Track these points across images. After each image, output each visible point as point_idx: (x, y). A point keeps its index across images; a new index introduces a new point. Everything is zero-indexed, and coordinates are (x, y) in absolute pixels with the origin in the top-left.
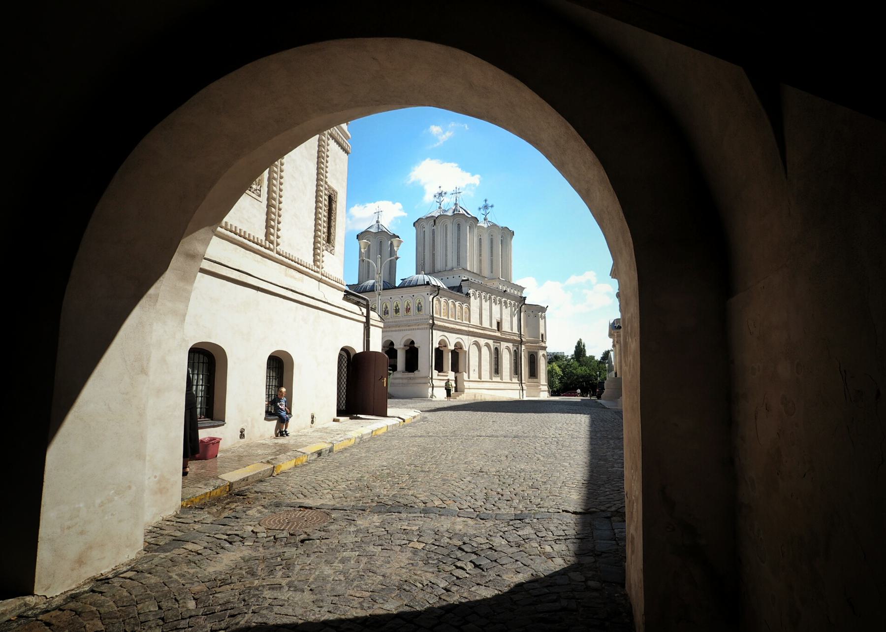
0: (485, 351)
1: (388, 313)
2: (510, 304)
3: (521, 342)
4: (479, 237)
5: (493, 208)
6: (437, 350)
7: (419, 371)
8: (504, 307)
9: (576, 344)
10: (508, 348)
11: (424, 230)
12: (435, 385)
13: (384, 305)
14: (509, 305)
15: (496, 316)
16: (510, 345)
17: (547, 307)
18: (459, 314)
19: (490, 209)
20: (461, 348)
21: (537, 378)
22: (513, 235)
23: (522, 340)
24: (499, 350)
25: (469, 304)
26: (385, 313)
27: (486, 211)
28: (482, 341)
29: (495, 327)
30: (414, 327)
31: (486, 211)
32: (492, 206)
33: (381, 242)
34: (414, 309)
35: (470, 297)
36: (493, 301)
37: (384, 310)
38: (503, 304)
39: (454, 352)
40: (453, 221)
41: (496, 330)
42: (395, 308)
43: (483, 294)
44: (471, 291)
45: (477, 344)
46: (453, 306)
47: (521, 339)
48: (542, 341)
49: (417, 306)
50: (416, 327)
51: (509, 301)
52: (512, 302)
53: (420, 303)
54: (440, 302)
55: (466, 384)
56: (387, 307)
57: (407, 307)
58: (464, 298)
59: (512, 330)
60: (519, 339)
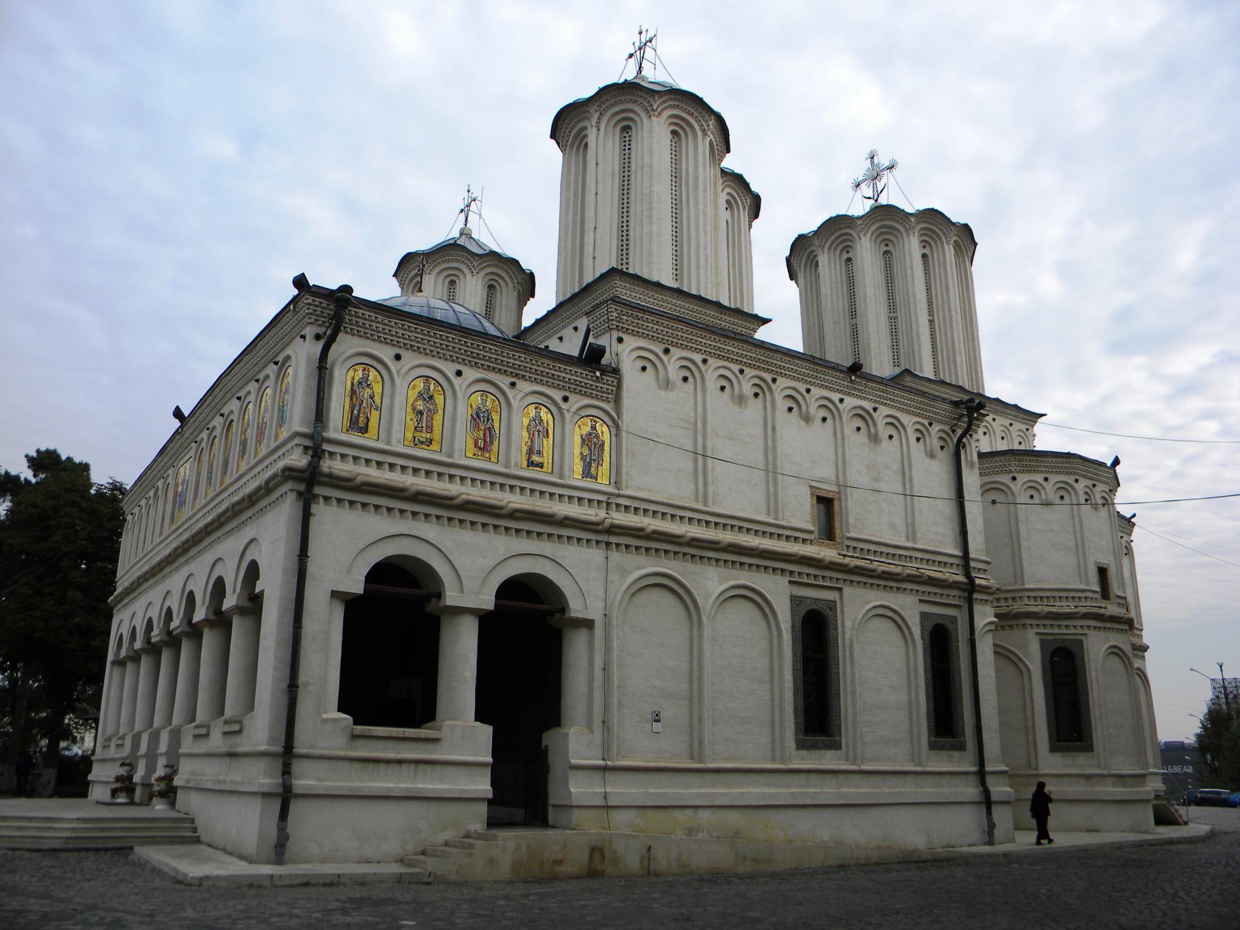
2: (894, 423)
3: (970, 590)
4: (845, 256)
14: (884, 432)
17: (1116, 462)
19: (886, 177)
21: (1089, 748)
23: (971, 580)
25: (617, 400)
27: (875, 187)
29: (801, 514)
31: (875, 187)
32: (891, 168)
38: (850, 425)
39: (486, 621)
40: (599, 118)
41: (812, 537)
47: (968, 575)
52: (907, 420)
55: (580, 789)
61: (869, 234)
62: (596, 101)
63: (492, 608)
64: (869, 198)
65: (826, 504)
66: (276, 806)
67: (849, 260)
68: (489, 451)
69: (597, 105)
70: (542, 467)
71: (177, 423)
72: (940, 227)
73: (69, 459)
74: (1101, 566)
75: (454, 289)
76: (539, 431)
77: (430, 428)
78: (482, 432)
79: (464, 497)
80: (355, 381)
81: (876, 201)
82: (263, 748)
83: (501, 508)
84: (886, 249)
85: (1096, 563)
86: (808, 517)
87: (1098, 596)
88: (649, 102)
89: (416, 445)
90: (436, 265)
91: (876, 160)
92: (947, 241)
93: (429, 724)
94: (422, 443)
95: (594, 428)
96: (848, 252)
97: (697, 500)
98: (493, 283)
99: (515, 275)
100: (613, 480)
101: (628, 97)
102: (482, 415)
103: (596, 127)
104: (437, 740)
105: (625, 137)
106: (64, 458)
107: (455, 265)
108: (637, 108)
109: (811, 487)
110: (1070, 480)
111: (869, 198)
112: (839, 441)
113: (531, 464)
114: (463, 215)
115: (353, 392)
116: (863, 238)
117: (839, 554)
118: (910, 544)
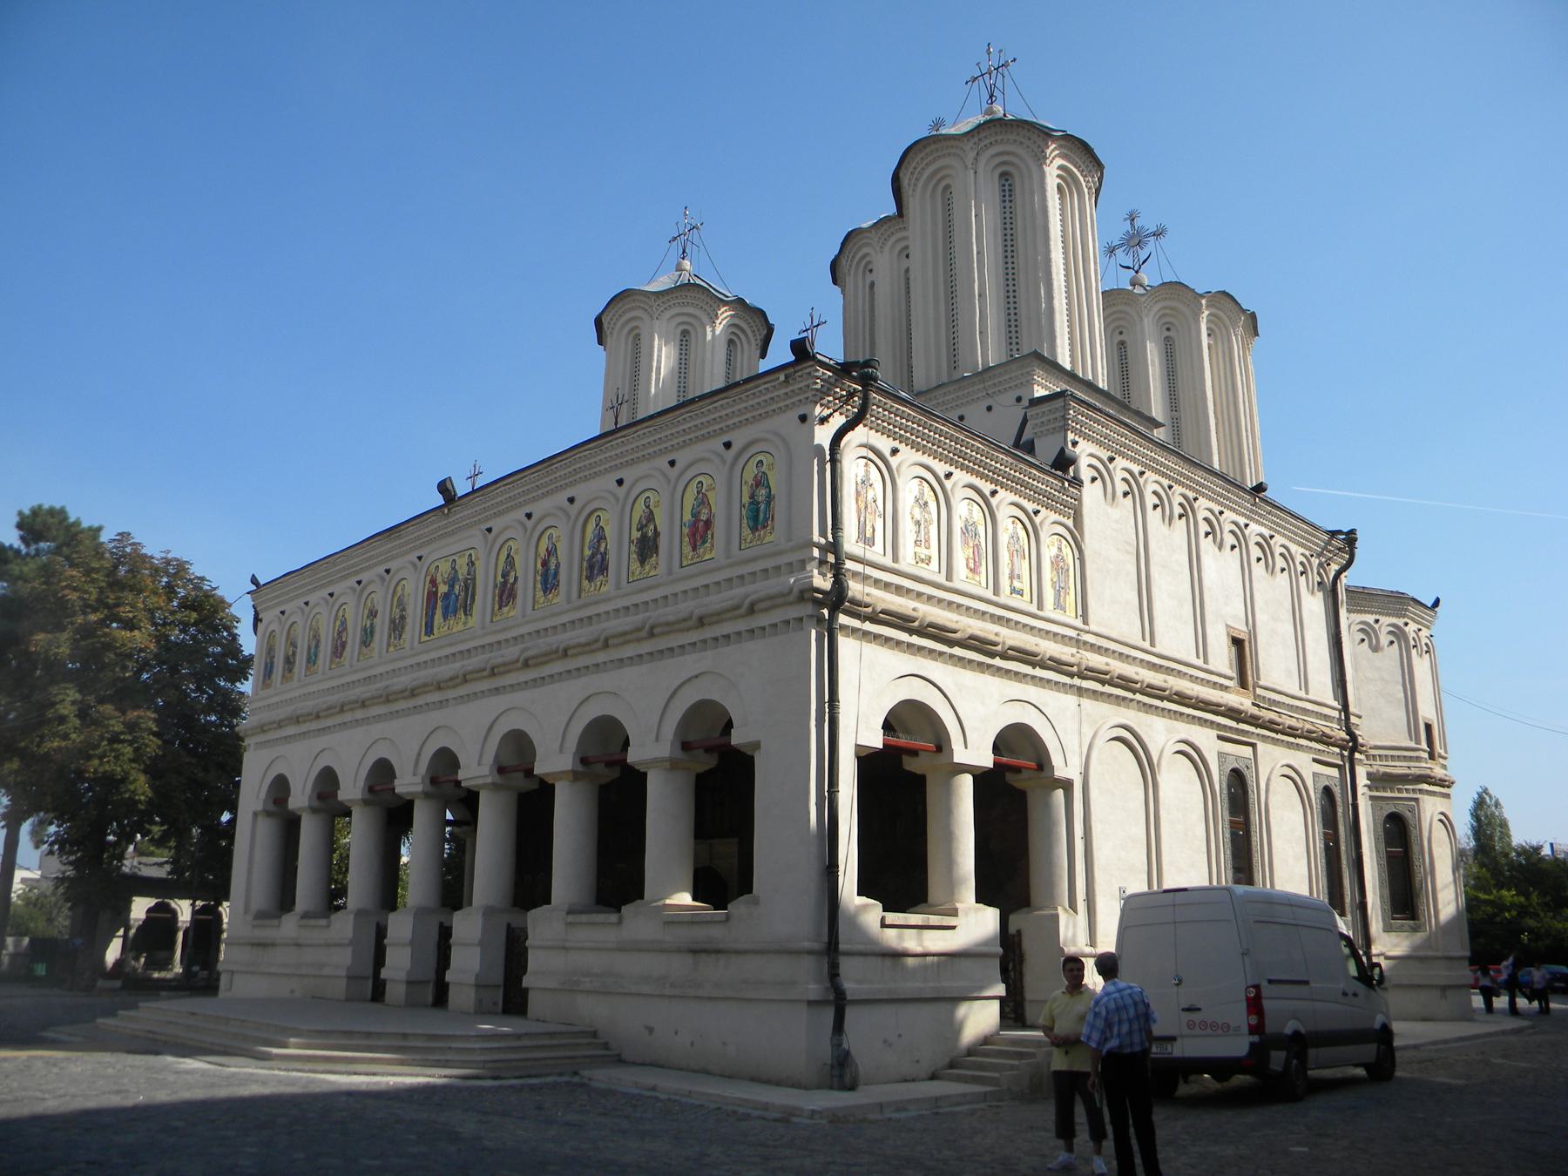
0: (1180, 785)
1: (604, 568)
2: (1288, 556)
3: (1352, 745)
4: (1119, 338)
5: (1162, 240)
6: (868, 761)
7: (756, 902)
8: (1258, 570)
9: (1470, 805)
10: (1294, 776)
11: (869, 278)
12: (849, 986)
13: (591, 527)
14: (1280, 563)
15: (1225, 613)
16: (1303, 762)
17: (1437, 603)
18: (1023, 567)
19: (1151, 245)
20: (1042, 762)
22: (1258, 335)
23: (1353, 737)
24: (1251, 782)
26: (591, 567)
28: (1161, 733)
29: (1222, 658)
30: (728, 628)
31: (1137, 255)
32: (1158, 234)
33: (685, 333)
34: (729, 519)
35: (1077, 482)
36: (1203, 527)
37: (588, 553)
38: (1256, 552)
39: (983, 779)
40: (976, 159)
42: (636, 535)
43: (1151, 483)
44: (1085, 452)
45: (1133, 743)
46: (977, 515)
47: (1350, 732)
48: (1432, 756)
49: (746, 499)
50: (742, 625)
51: (1279, 539)
52: (1294, 548)
53: (761, 482)
54: (890, 477)
56: (601, 537)
57: (695, 515)
58: (1048, 483)
59: (1305, 683)
60: (1343, 735)
61: (1152, 313)
62: (973, 136)
63: (991, 765)
64: (1128, 268)
65: (1237, 643)
66: (829, 1015)
67: (1122, 343)
68: (979, 573)
69: (973, 141)
70: (1022, 595)
71: (439, 500)
72: (1228, 314)
73: (77, 523)
74: (1427, 721)
75: (687, 341)
76: (1017, 551)
77: (927, 541)
78: (971, 550)
79: (970, 631)
80: (859, 482)
81: (1137, 272)
82: (807, 945)
83: (995, 644)
84: (1167, 333)
85: (1424, 718)
86: (1227, 662)
87: (1426, 755)
88: (1039, 147)
89: (917, 563)
90: (665, 309)
91: (1138, 223)
92: (1234, 332)
93: (918, 908)
94: (922, 561)
95: (1060, 549)
96: (1121, 333)
97: (1144, 640)
98: (735, 338)
99: (758, 330)
100: (1080, 612)
101: (1012, 137)
102: (970, 528)
103: (972, 169)
104: (953, 928)
105: (1004, 185)
106: (72, 519)
107: (691, 310)
108: (1020, 151)
109: (1227, 626)
110: (1400, 622)
111: (1128, 268)
112: (1246, 569)
113: (1013, 591)
114: (676, 248)
115: (858, 493)
116: (1146, 321)
117: (1254, 704)
118: (1302, 694)
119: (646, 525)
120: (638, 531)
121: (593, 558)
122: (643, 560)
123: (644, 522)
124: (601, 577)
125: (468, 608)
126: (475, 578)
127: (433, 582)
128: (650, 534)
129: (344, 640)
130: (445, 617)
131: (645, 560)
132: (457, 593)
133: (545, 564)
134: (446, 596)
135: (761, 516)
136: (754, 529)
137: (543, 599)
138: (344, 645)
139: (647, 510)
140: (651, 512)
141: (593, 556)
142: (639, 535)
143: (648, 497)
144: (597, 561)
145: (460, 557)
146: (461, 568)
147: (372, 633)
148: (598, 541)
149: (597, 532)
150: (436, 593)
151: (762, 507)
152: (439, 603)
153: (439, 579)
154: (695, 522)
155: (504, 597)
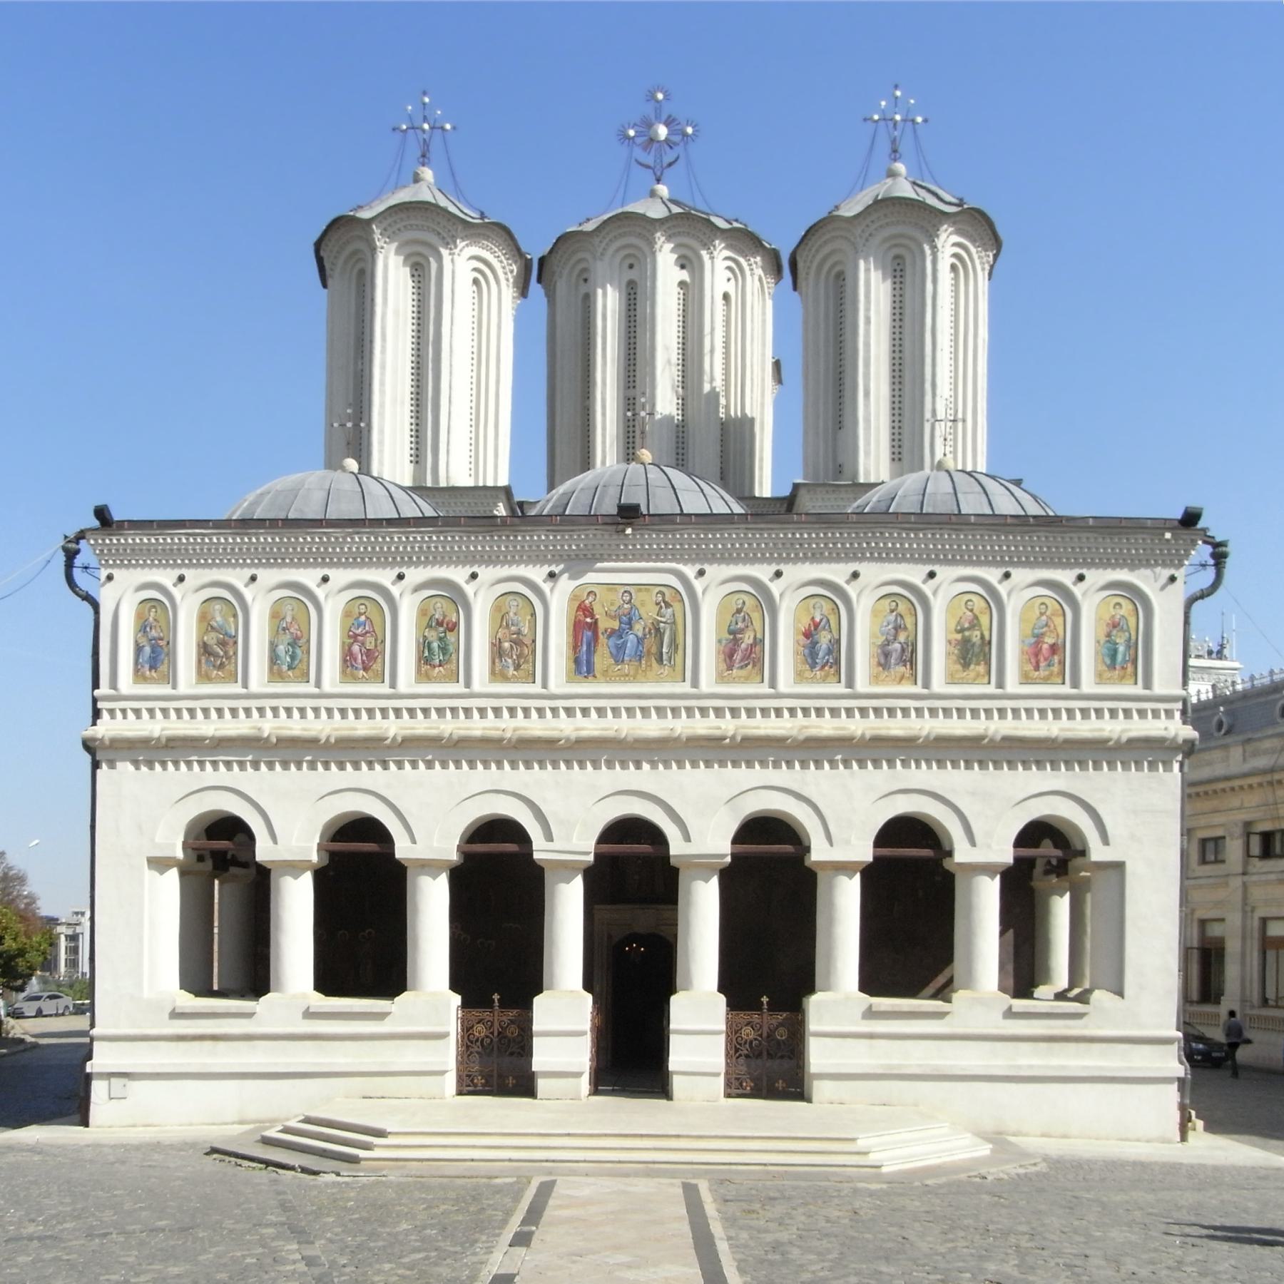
26: (887, 655)
119: (968, 629)
120: (959, 632)
121: (888, 645)
122: (966, 665)
123: (966, 625)
124: (903, 669)
125: (665, 657)
126: (674, 623)
127: (585, 610)
128: (975, 636)
129: (370, 644)
130: (618, 655)
131: (969, 665)
132: (640, 634)
133: (807, 635)
134: (612, 633)
135: (1120, 657)
136: (1112, 666)
137: (808, 674)
138: (371, 657)
139: (970, 613)
140: (976, 617)
141: (888, 643)
142: (959, 636)
143: (970, 600)
144: (896, 651)
145: (640, 590)
146: (643, 605)
147: (444, 649)
148: (897, 628)
149: (892, 617)
150: (594, 626)
151: (1121, 649)
152: (602, 639)
153: (599, 612)
154: (1037, 643)
155: (738, 657)
